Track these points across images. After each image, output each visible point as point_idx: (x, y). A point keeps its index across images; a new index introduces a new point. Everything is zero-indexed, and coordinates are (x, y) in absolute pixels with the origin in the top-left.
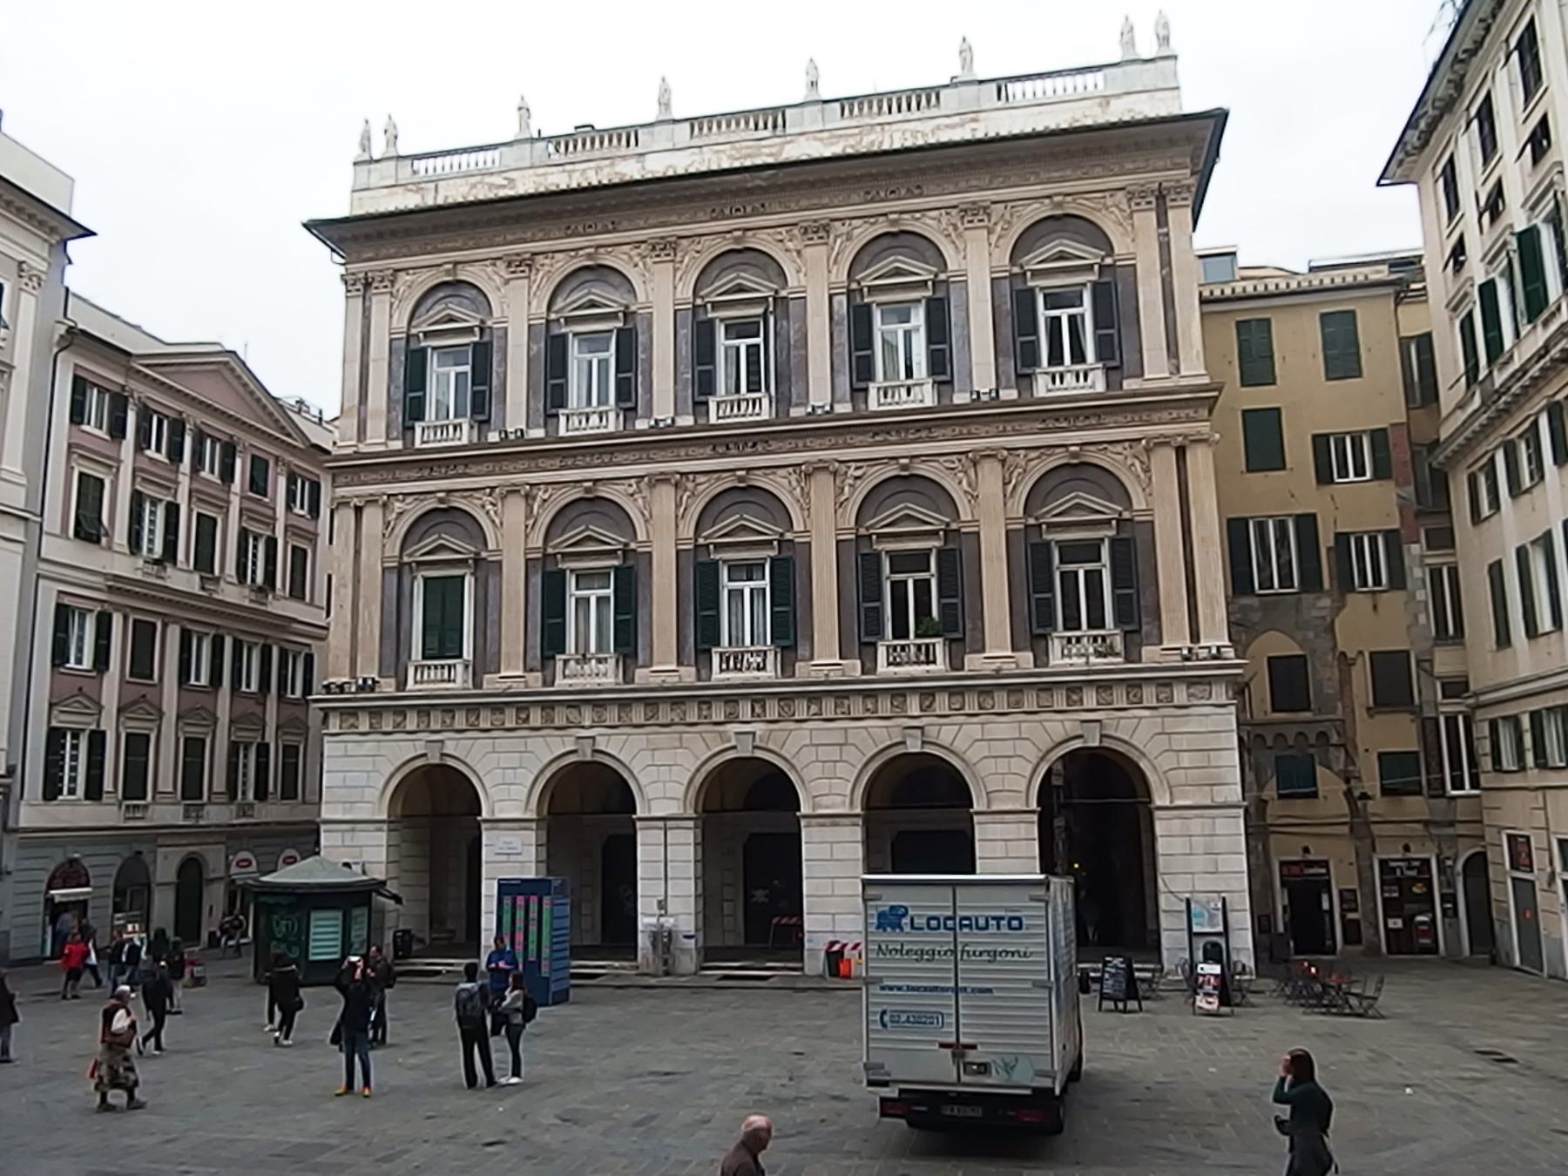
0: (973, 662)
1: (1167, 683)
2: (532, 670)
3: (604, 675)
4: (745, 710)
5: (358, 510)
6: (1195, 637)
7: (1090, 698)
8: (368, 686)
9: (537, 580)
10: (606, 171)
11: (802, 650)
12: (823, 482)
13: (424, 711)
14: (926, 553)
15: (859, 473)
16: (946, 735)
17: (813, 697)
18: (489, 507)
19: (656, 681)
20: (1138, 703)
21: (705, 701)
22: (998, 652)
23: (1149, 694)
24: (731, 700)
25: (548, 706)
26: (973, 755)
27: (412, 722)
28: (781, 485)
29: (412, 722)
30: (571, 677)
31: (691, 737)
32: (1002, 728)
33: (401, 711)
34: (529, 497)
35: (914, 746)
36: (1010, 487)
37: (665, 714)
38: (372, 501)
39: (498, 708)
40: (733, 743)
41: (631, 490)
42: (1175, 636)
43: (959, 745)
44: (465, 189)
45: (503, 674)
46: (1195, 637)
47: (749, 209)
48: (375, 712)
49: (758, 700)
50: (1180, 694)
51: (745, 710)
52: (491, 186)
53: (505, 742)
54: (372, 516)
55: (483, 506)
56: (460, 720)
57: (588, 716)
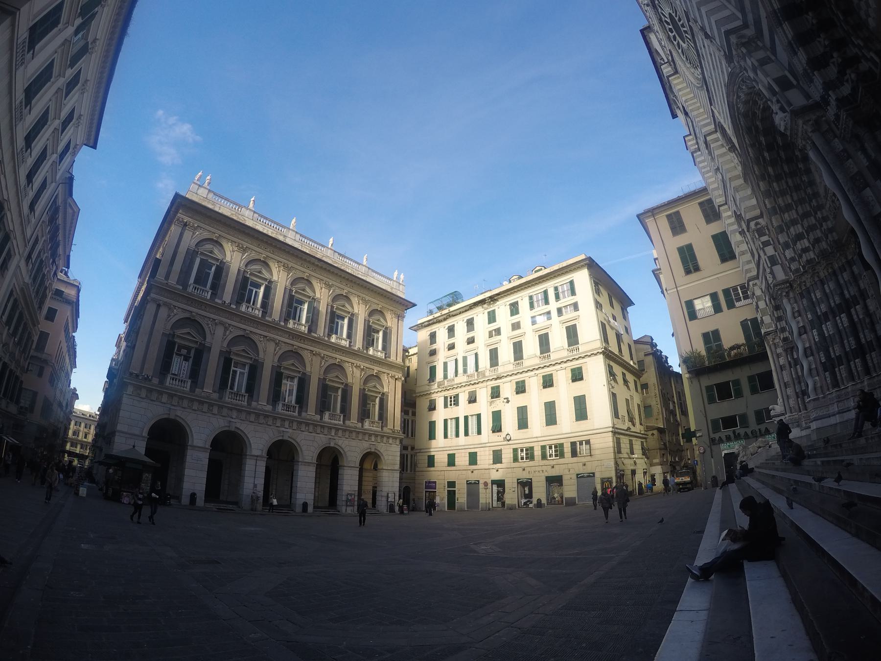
0: (347, 422)
1: (388, 438)
2: (214, 391)
4: (287, 424)
5: (159, 306)
7: (373, 439)
8: (147, 379)
9: (222, 359)
11: (304, 409)
13: (171, 396)
16: (340, 443)
17: (307, 424)
19: (259, 407)
20: (382, 441)
21: (275, 418)
23: (385, 439)
24: (283, 420)
25: (221, 407)
26: (346, 450)
27: (165, 398)
28: (306, 356)
29: (165, 398)
32: (354, 443)
33: (161, 393)
34: (226, 329)
35: (332, 445)
37: (262, 420)
38: (165, 304)
39: (201, 403)
42: (390, 426)
43: (343, 446)
48: (150, 391)
49: (292, 422)
50: (391, 441)
51: (287, 424)
54: (163, 312)
55: (208, 324)
56: (185, 403)
57: (234, 414)
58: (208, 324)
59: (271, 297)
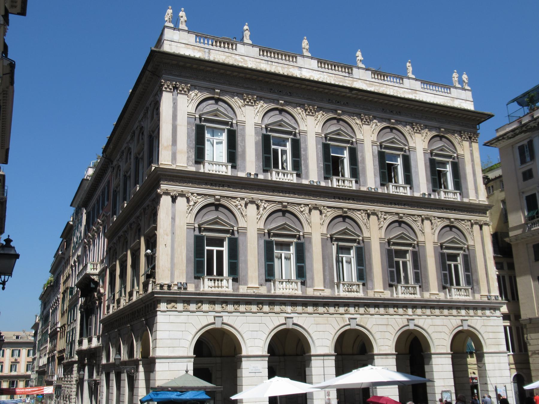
3: (294, 289)
6: (489, 291)
10: (286, 69)
12: (373, 218)
14: (406, 252)
15: (385, 217)
18: (240, 207)
22: (434, 291)
30: (281, 289)
31: (332, 319)
32: (438, 321)
36: (433, 230)
40: (348, 323)
41: (302, 210)
42: (484, 292)
44: (224, 57)
45: (249, 286)
46: (489, 291)
47: (342, 103)
52: (236, 60)
53: (251, 318)
54: (181, 201)
58: (236, 206)
59: (303, 153)
